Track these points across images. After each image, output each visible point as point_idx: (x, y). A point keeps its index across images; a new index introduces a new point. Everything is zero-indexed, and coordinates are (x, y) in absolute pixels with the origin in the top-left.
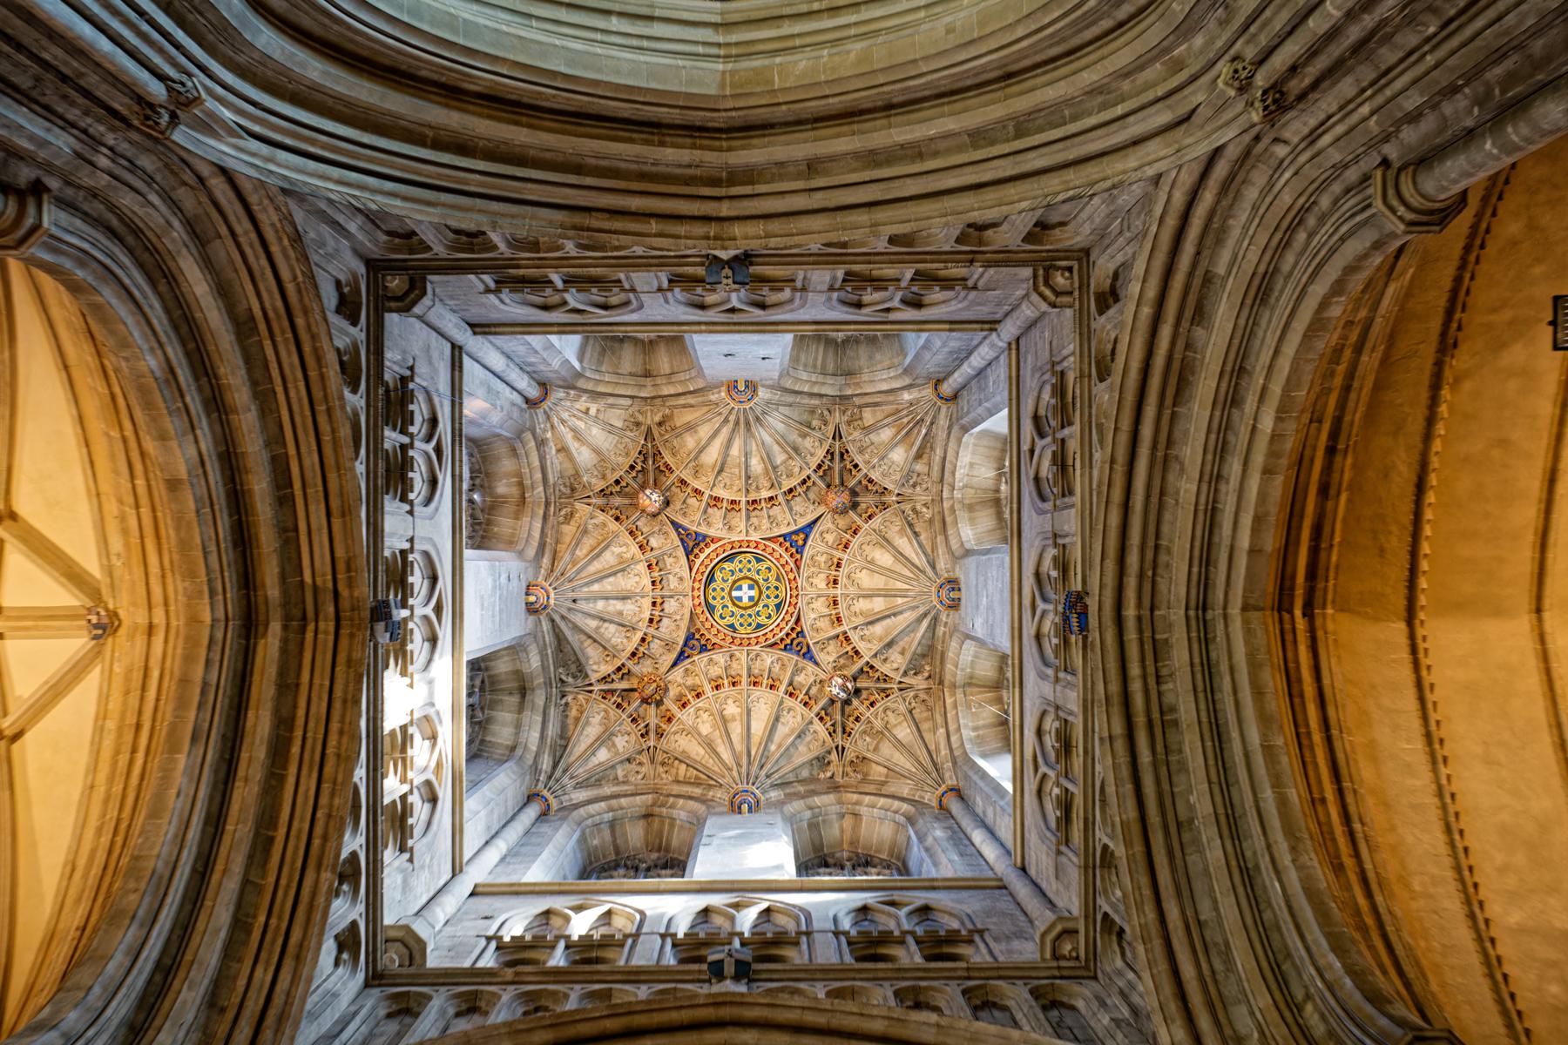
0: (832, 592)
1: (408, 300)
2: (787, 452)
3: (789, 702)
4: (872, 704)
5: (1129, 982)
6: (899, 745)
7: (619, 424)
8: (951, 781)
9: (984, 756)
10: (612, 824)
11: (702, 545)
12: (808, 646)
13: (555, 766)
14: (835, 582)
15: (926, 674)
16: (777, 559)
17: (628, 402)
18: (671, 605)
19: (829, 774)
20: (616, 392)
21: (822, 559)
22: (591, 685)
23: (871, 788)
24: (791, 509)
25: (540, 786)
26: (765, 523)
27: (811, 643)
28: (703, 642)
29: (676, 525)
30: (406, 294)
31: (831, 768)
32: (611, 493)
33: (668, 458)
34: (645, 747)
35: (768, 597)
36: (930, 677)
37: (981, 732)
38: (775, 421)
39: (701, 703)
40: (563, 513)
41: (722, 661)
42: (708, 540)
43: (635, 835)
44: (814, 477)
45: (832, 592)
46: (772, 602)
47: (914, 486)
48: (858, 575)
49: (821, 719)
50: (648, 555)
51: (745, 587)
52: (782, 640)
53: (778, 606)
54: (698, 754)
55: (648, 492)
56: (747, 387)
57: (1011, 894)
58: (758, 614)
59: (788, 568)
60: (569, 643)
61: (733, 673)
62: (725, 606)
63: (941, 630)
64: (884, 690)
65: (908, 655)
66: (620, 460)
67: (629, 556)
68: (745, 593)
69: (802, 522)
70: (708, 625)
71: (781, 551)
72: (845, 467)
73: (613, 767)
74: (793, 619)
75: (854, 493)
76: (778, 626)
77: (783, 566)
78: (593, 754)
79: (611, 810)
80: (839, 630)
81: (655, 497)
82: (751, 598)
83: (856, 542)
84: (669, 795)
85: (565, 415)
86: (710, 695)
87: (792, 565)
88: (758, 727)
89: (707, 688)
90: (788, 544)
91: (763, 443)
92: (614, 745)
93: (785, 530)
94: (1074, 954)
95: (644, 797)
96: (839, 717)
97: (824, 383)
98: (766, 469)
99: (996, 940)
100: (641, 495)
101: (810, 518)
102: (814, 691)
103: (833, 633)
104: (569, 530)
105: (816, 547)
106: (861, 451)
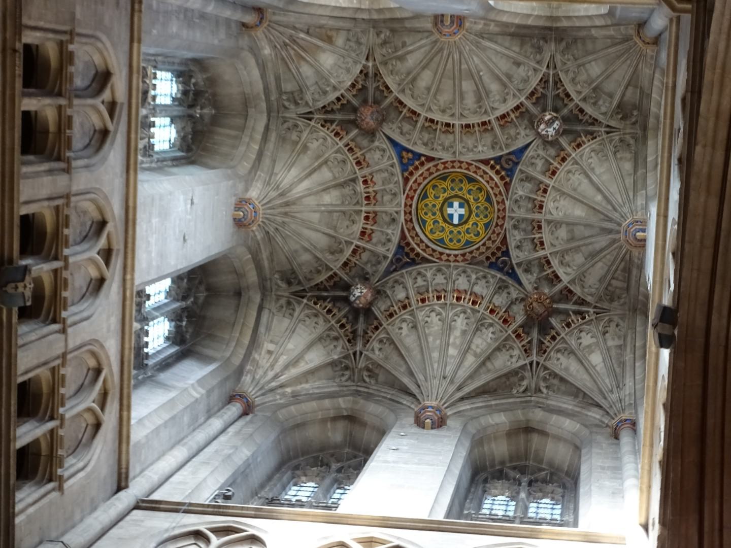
0: (457, 129)
2: (320, 166)
3: (561, 174)
7: (286, 322)
11: (407, 249)
12: (510, 154)
15: (542, 42)
16: (425, 178)
18: (462, 283)
19: (632, 142)
21: (426, 136)
27: (506, 151)
28: (499, 254)
32: (354, 332)
33: (323, 277)
44: (344, 141)
45: (457, 129)
48: (442, 103)
50: (413, 302)
51: (450, 211)
52: (502, 178)
55: (352, 299)
59: (433, 170)
61: (530, 228)
62: (468, 231)
63: (492, 28)
68: (456, 211)
69: (391, 152)
70: (483, 249)
71: (417, 175)
72: (338, 109)
74: (483, 167)
77: (431, 174)
80: (495, 124)
83: (410, 103)
87: (431, 164)
90: (411, 168)
92: (589, 346)
93: (398, 170)
96: (579, 128)
101: (386, 145)
103: (498, 130)
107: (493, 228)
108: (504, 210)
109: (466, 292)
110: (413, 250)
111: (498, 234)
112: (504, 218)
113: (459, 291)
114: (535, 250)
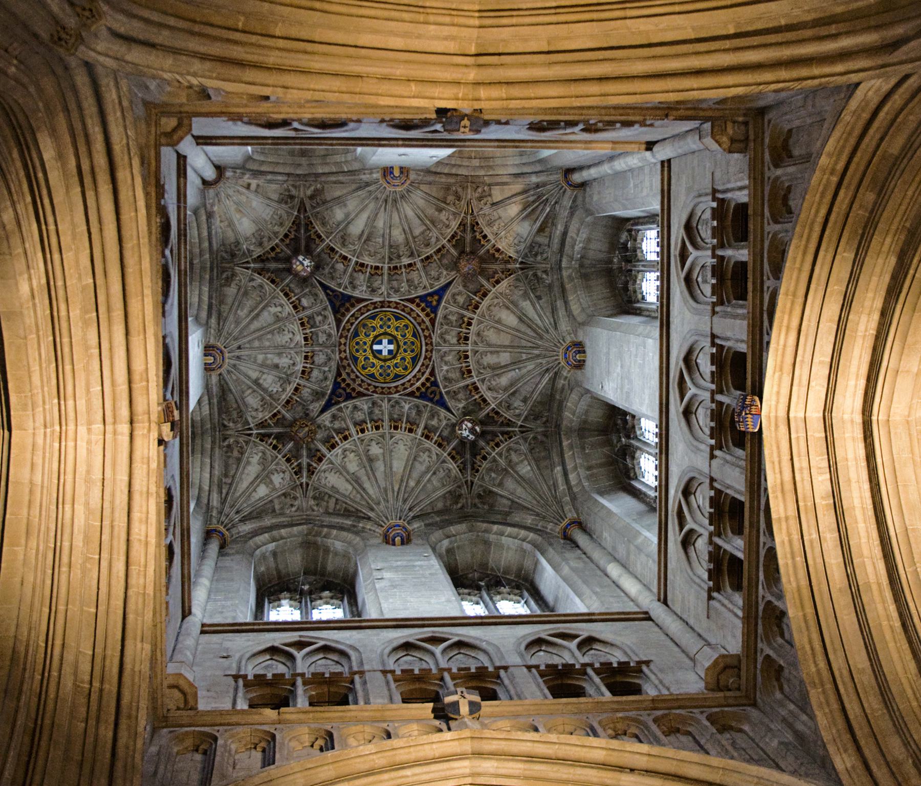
1: (175, 137)
3: (428, 444)
4: (498, 445)
5: (791, 712)
6: (522, 480)
7: (275, 197)
8: (571, 515)
9: (601, 494)
10: (274, 554)
11: (348, 305)
12: (441, 393)
13: (223, 502)
14: (467, 339)
15: (544, 419)
16: (415, 318)
17: (285, 178)
18: (320, 358)
19: (459, 505)
20: (276, 170)
21: (453, 318)
22: (250, 429)
23: (499, 517)
24: (427, 274)
25: (214, 521)
26: (404, 286)
27: (443, 391)
28: (348, 391)
29: (325, 288)
30: (175, 130)
31: (462, 501)
33: (319, 228)
34: (298, 483)
35: (405, 351)
36: (547, 421)
37: (595, 471)
38: (418, 198)
39: (346, 445)
40: (224, 276)
41: (365, 407)
42: (353, 301)
43: (295, 561)
44: (448, 246)
46: (409, 356)
47: (536, 255)
49: (453, 458)
51: (385, 341)
52: (418, 389)
53: (415, 360)
54: (346, 490)
55: (301, 258)
56: (401, 172)
57: (657, 625)
58: (396, 366)
60: (232, 393)
61: (375, 418)
62: (366, 358)
63: (561, 382)
64: (507, 433)
65: (530, 403)
66: (276, 228)
67: (284, 315)
68: (385, 347)
69: (438, 285)
70: (353, 376)
73: (271, 501)
75: (482, 260)
76: (415, 377)
77: (419, 324)
78: (255, 490)
79: (274, 540)
80: (469, 381)
81: (307, 262)
82: (390, 352)
84: (323, 526)
85: (230, 192)
86: (356, 437)
87: (428, 323)
88: (398, 466)
89: (353, 430)
91: (406, 216)
92: (271, 482)
93: (421, 293)
94: (736, 686)
95: (300, 528)
96: (468, 456)
97: (460, 166)
98: (407, 239)
99: (661, 671)
100: (294, 261)
101: (443, 281)
102: (445, 433)
103: (462, 384)
104: (231, 291)
105: (447, 308)
106: (490, 224)
107: (374, 384)
108: (390, 393)
109: (313, 363)
110: (348, 310)
111: (367, 389)
112: (382, 393)
113: (312, 357)
114: (355, 424)
